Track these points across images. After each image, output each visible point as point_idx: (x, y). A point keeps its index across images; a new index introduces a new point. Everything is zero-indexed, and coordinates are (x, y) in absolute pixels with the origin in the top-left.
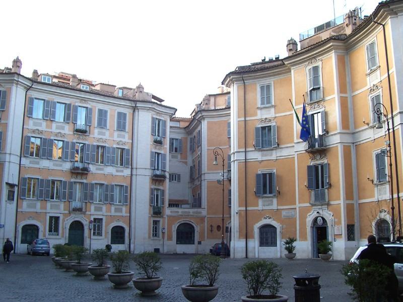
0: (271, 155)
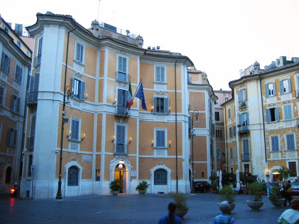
0: (79, 106)
